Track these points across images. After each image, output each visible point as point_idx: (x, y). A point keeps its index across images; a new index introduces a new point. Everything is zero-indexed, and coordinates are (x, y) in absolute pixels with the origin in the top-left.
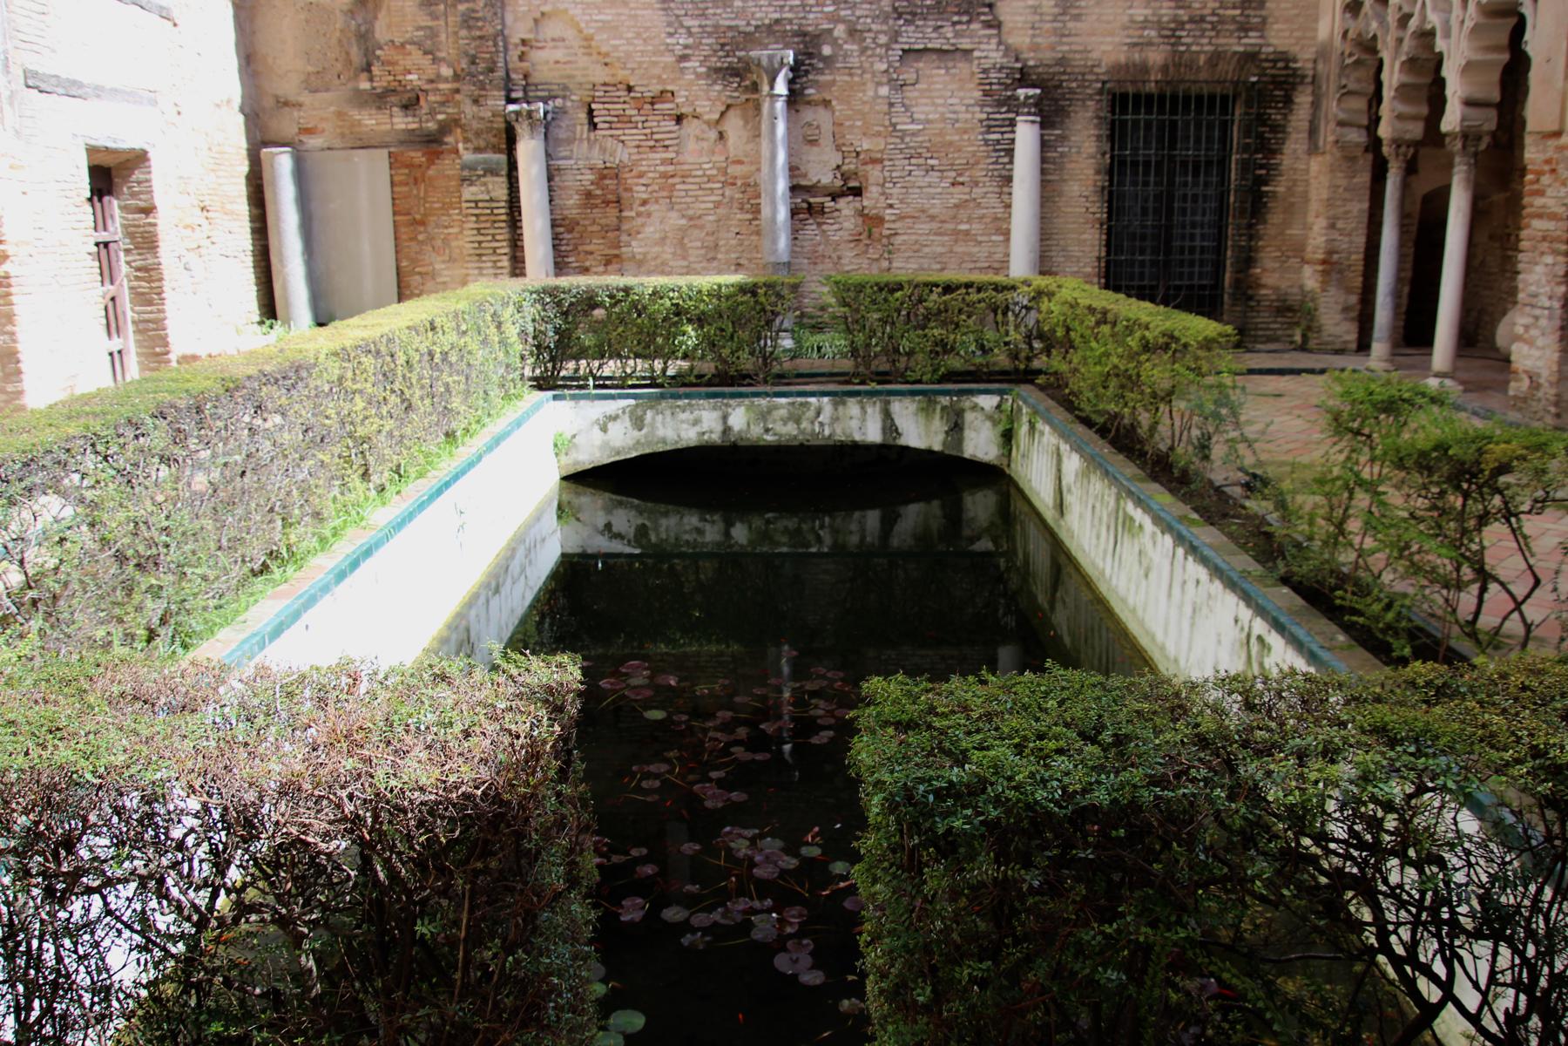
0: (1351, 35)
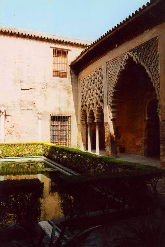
0: (82, 109)
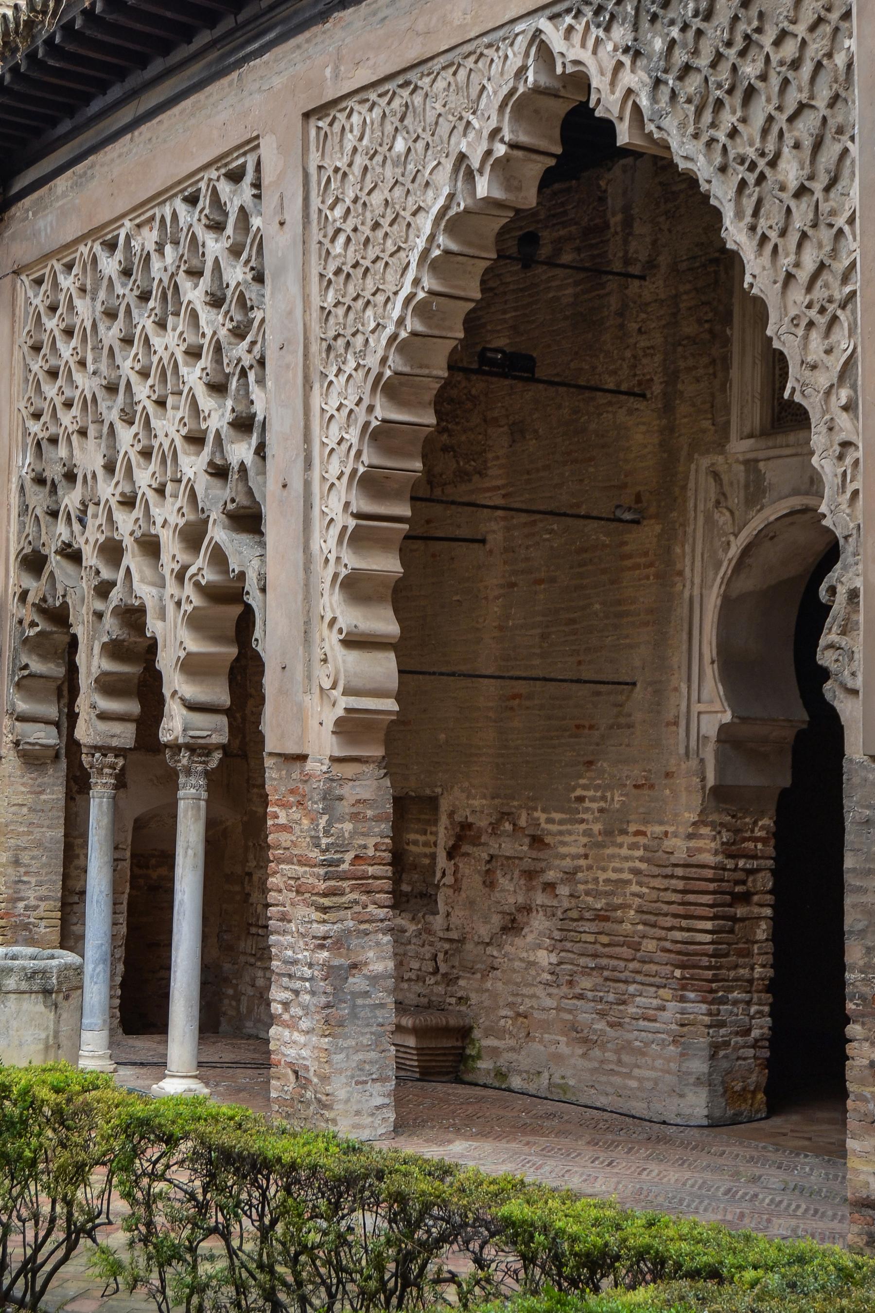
0: (31, 598)
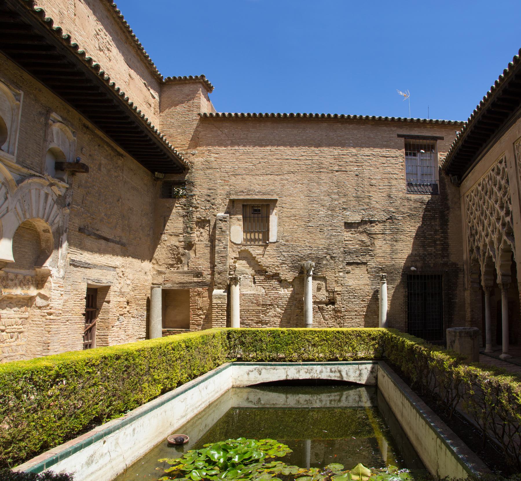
0: (472, 258)
